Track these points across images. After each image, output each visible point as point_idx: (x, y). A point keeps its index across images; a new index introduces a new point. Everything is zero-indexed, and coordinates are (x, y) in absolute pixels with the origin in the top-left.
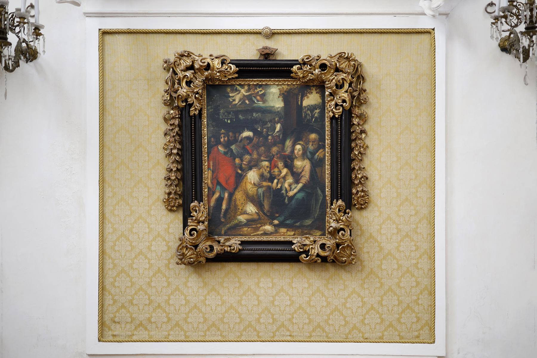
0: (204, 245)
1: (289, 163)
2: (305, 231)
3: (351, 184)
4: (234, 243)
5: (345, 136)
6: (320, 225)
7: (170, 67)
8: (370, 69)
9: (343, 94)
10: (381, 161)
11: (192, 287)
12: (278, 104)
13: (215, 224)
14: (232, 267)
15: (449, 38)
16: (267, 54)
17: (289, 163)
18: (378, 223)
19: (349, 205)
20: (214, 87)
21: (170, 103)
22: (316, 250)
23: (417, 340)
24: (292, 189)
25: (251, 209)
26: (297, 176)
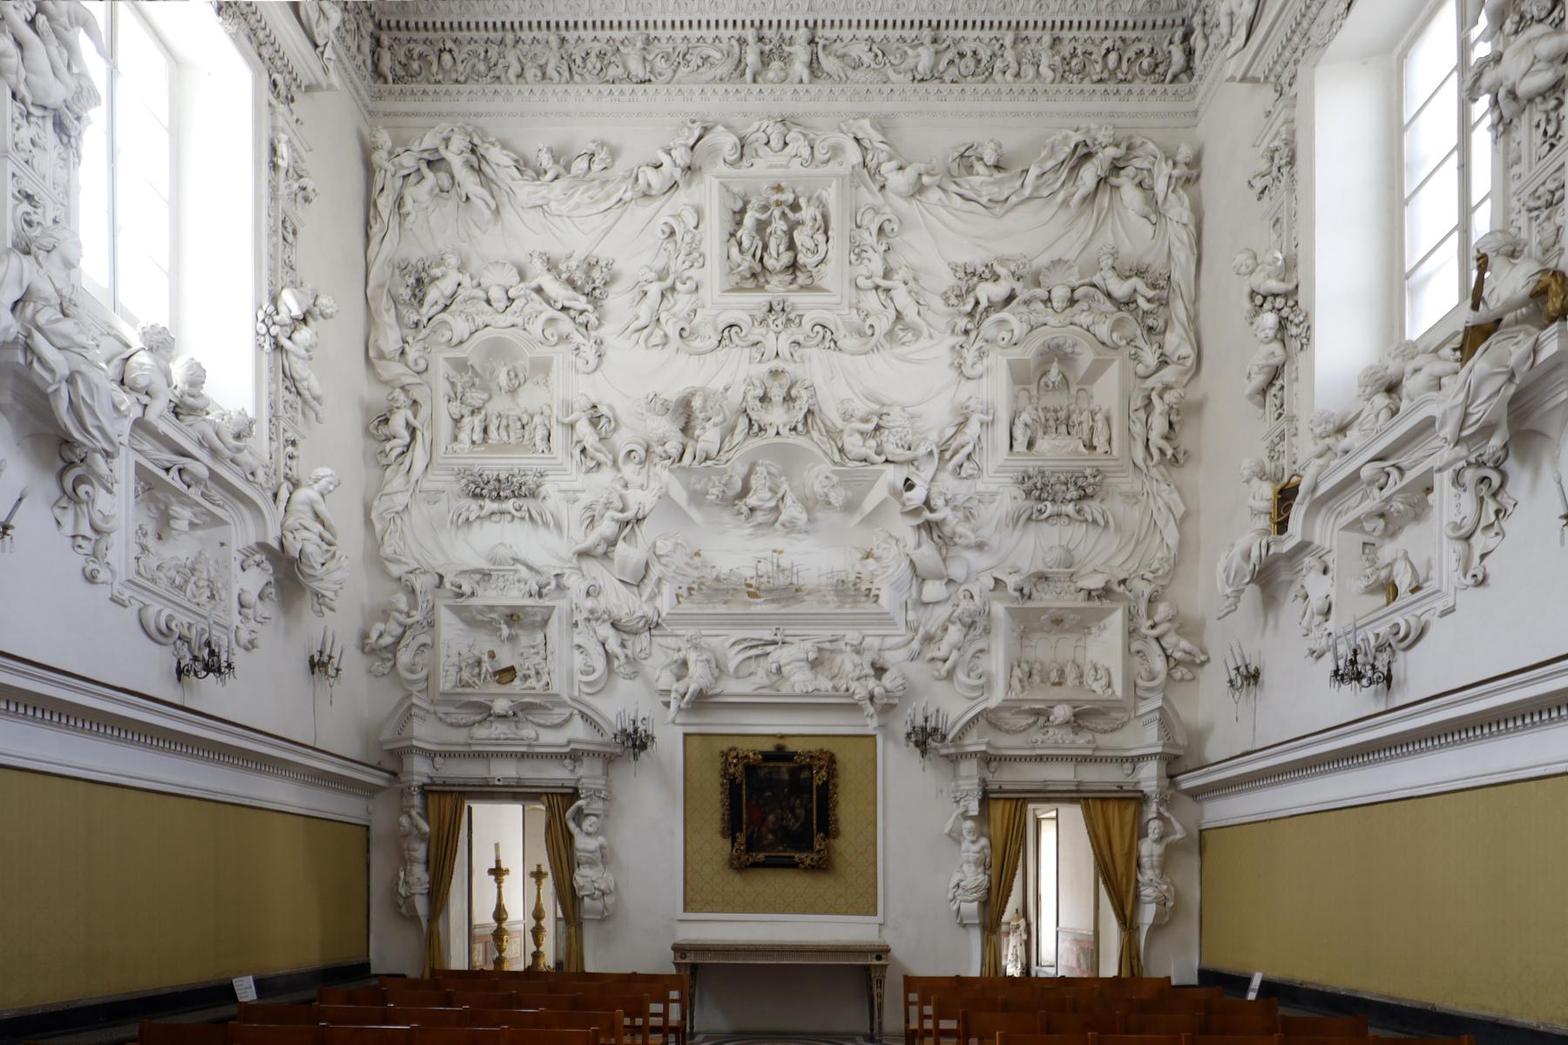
0: (744, 858)
1: (792, 810)
2: (800, 849)
3: (828, 823)
4: (761, 856)
5: (826, 796)
6: (810, 848)
7: (725, 755)
8: (839, 757)
9: (823, 773)
10: (846, 811)
11: (736, 881)
12: (786, 777)
13: (751, 846)
14: (759, 870)
15: (885, 739)
16: (780, 748)
17: (792, 810)
18: (845, 846)
19: (827, 835)
20: (750, 769)
21: (724, 776)
22: (808, 861)
23: (867, 914)
24: (794, 826)
25: (770, 837)
26: (797, 819)
